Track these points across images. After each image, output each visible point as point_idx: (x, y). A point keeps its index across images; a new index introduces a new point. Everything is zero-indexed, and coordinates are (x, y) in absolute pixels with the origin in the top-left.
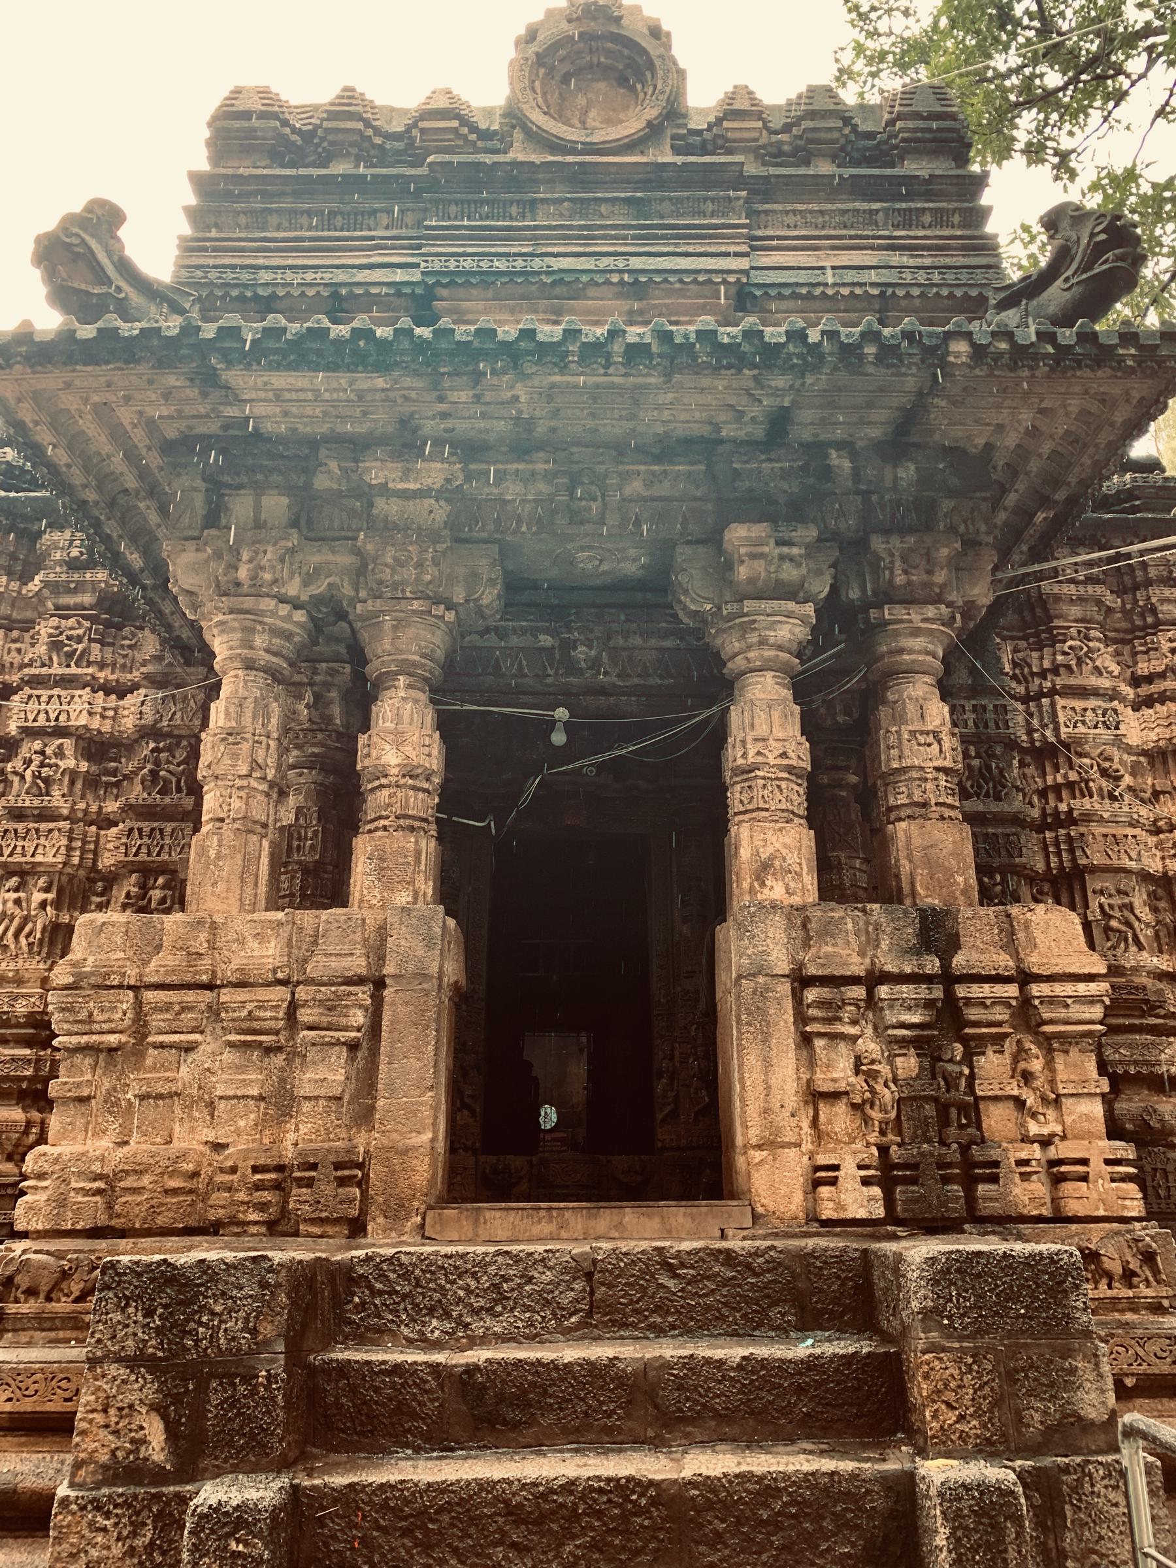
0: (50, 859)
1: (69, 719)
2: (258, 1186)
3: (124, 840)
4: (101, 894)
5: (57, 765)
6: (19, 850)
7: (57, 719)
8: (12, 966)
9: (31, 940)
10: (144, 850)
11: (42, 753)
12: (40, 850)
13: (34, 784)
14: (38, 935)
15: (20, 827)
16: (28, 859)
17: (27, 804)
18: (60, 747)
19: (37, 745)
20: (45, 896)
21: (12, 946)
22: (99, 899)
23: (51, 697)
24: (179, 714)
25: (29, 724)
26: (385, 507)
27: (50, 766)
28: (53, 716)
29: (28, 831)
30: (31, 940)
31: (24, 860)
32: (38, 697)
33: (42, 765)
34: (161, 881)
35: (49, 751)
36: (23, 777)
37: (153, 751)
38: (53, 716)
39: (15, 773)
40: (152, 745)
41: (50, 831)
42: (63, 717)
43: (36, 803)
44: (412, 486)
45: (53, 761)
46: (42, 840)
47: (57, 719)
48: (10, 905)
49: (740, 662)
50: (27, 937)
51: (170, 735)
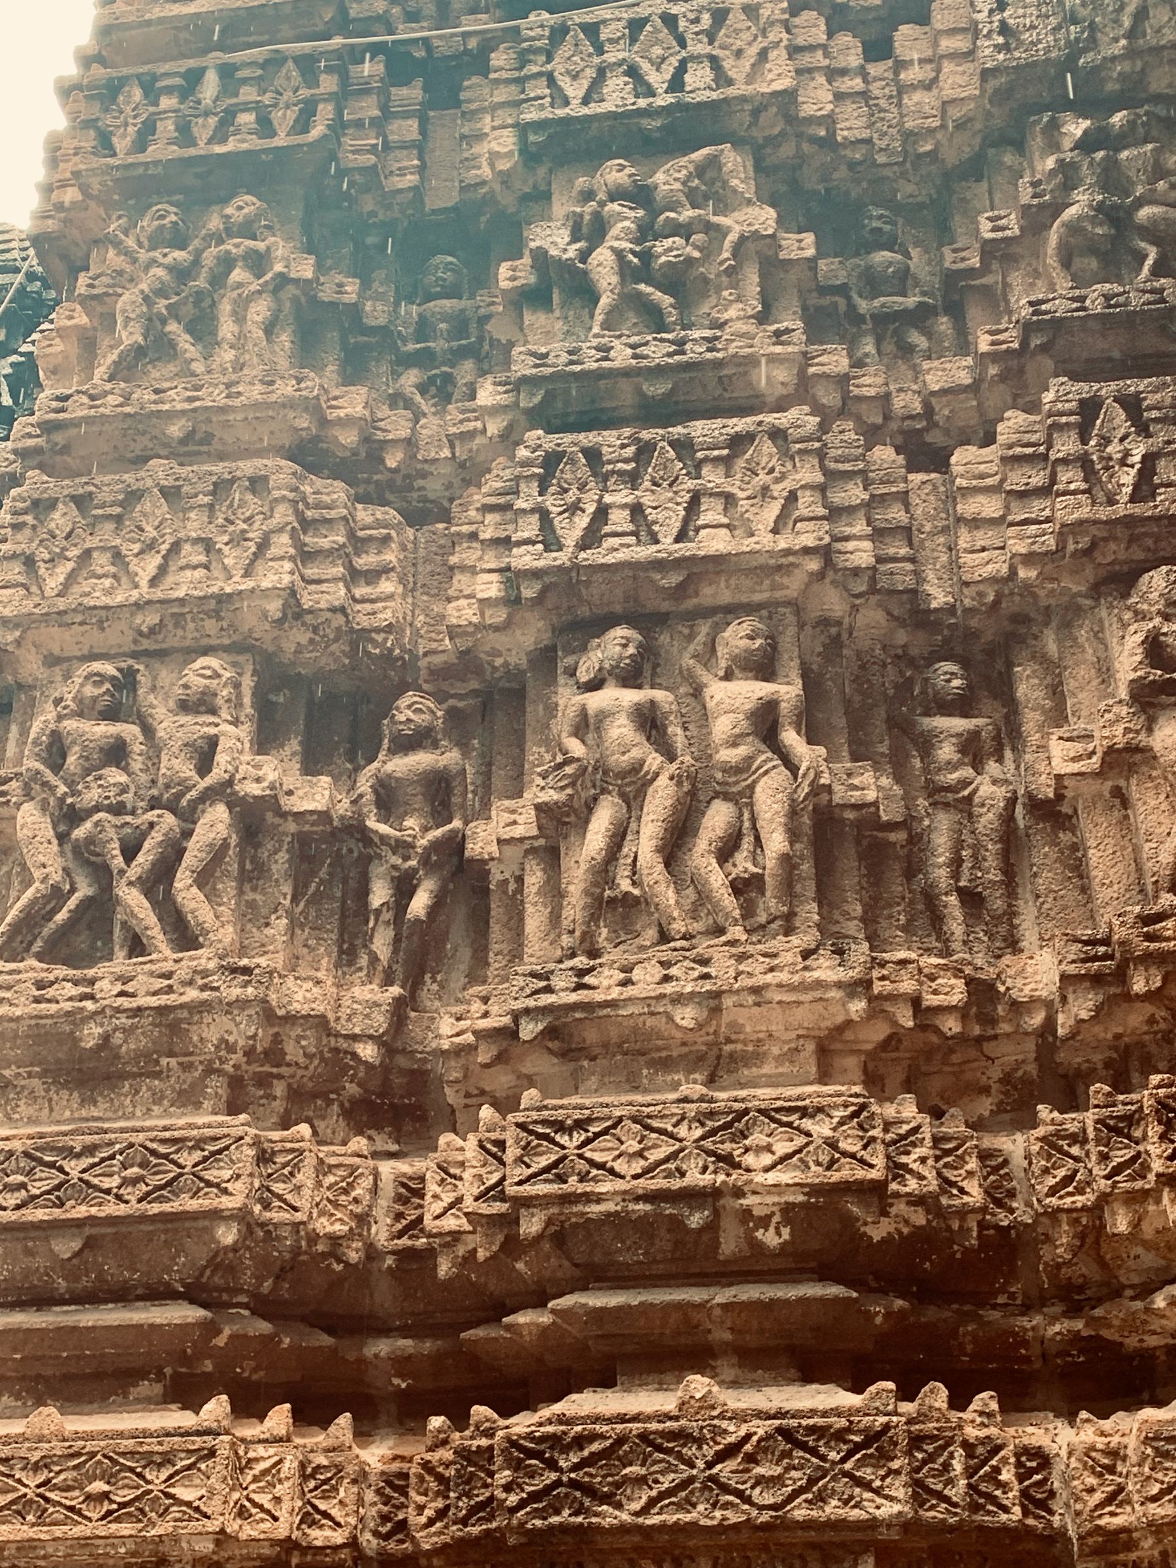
0: (764, 540)
1: (722, 78)
3: (1066, 446)
4: (962, 706)
5: (708, 227)
6: (619, 519)
7: (676, 83)
8: (686, 981)
9: (743, 864)
12: (711, 513)
13: (631, 302)
14: (776, 842)
15: (610, 441)
16: (668, 546)
17: (621, 356)
18: (709, 170)
19: (616, 173)
20: (762, 689)
21: (667, 896)
22: (959, 724)
25: (576, 109)
27: (684, 231)
28: (658, 79)
29: (645, 451)
30: (743, 864)
31: (645, 552)
32: (591, 30)
33: (646, 232)
37: (1085, 145)
38: (658, 79)
40: (1076, 128)
41: (739, 443)
42: (698, 78)
43: (657, 352)
45: (688, 214)
46: (712, 477)
47: (676, 83)
48: (621, 730)
50: (726, 851)
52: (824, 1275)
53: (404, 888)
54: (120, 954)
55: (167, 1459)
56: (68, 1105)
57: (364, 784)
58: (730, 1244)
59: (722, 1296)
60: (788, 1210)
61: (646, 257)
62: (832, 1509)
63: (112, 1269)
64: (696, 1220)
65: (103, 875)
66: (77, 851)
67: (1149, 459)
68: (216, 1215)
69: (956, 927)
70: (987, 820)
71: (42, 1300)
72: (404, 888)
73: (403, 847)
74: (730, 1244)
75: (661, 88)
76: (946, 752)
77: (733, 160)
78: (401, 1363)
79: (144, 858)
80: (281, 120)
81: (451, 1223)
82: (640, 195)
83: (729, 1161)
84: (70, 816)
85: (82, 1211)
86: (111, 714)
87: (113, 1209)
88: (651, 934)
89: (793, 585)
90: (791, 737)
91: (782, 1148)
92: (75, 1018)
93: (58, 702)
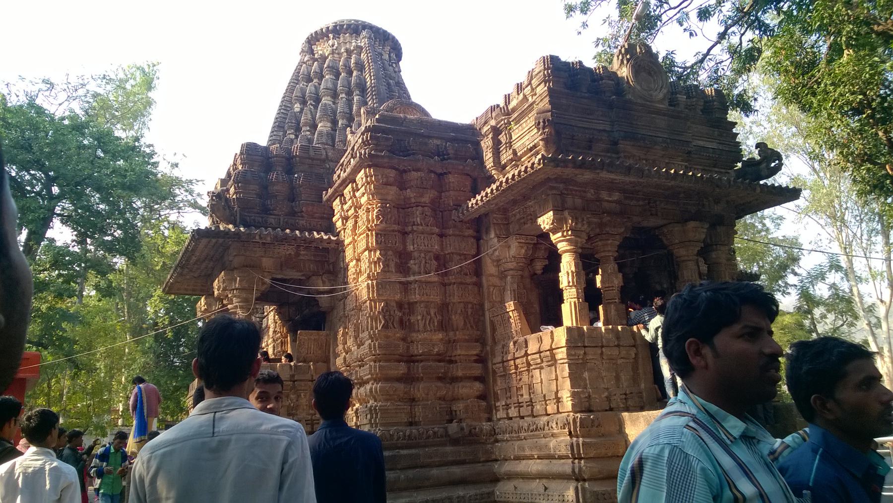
2: (621, 399)
11: (425, 258)
23: (424, 237)
26: (605, 204)
34: (470, 306)
35: (427, 258)
44: (610, 199)
80: (394, 242)
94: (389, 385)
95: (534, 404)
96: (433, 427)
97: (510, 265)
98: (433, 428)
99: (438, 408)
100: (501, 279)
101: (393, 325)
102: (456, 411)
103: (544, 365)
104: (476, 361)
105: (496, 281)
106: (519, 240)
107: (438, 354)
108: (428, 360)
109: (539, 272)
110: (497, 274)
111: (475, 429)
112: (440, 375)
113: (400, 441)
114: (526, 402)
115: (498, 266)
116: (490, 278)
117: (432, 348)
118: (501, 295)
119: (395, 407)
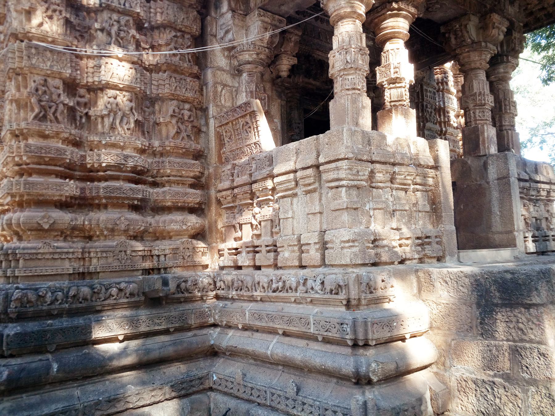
5: (128, 32)
7: (124, 5)
10: (178, 88)
11: (118, 22)
24: (186, 20)
36: (109, 34)
39: (102, 30)
49: (473, 65)
51: (180, 31)
52: (133, 173)
53: (81, 117)
54: (49, 123)
55: (63, 185)
56: (41, 140)
57: (76, 102)
58: (124, 169)
59: (124, 174)
60: (131, 167)
61: (119, 33)
62: (135, 196)
63: (50, 162)
64: (122, 167)
65: (46, 111)
66: (41, 106)
67: (176, 86)
68: (66, 158)
69: (146, 135)
70: (151, 123)
71: (40, 164)
72: (81, 117)
73: (81, 112)
74: (124, 169)
75: (122, 4)
76: (147, 114)
77: (131, 19)
78: (79, 176)
79: (53, 110)
81: (90, 162)
82: (118, 22)
83: (126, 161)
84: (40, 101)
85: (49, 155)
86: (43, 86)
87: (53, 156)
88: (117, 133)
89: (135, 90)
90: (134, 111)
91: (132, 160)
92: (45, 130)
93: (34, 81)
94: (43, 214)
95: (279, 250)
96: (118, 280)
97: (246, 57)
98: (119, 283)
99: (128, 252)
100: (233, 76)
101: (56, 118)
102: (158, 256)
103: (299, 191)
104: (192, 186)
105: (227, 78)
106: (262, 18)
107: (134, 170)
108: (117, 178)
109: (284, 74)
110: (228, 68)
111: (186, 281)
112: (136, 202)
113: (57, 305)
114: (267, 246)
115: (230, 57)
116: (219, 72)
117: (123, 162)
118: (233, 98)
119: (51, 250)
